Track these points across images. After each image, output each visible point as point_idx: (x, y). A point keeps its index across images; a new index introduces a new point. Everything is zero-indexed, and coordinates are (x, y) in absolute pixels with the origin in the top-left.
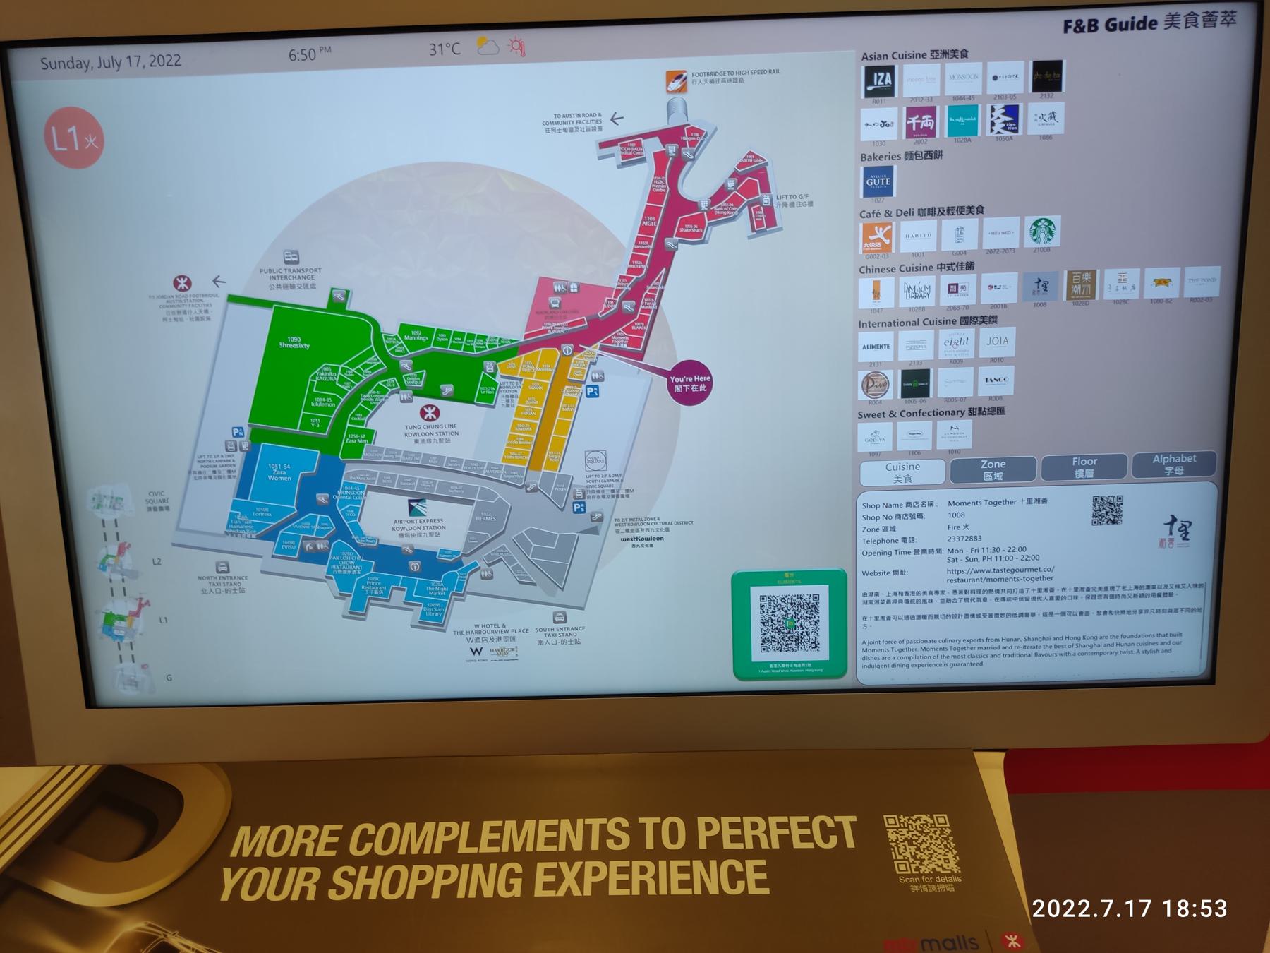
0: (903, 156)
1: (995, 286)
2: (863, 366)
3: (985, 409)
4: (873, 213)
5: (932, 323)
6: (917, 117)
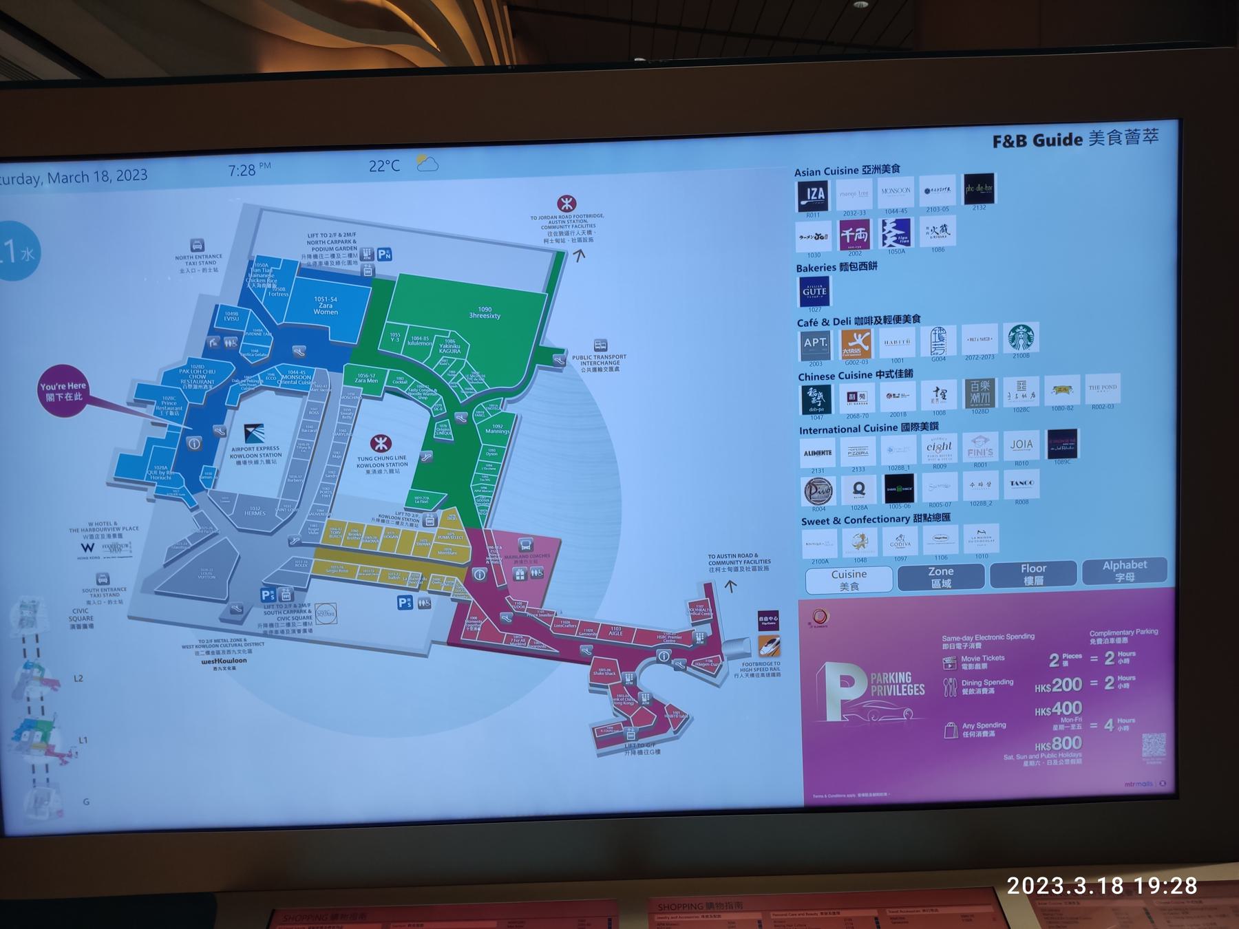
0: (838, 267)
1: (894, 395)
2: (804, 472)
3: (930, 515)
4: (811, 322)
5: (873, 429)
6: (851, 229)
